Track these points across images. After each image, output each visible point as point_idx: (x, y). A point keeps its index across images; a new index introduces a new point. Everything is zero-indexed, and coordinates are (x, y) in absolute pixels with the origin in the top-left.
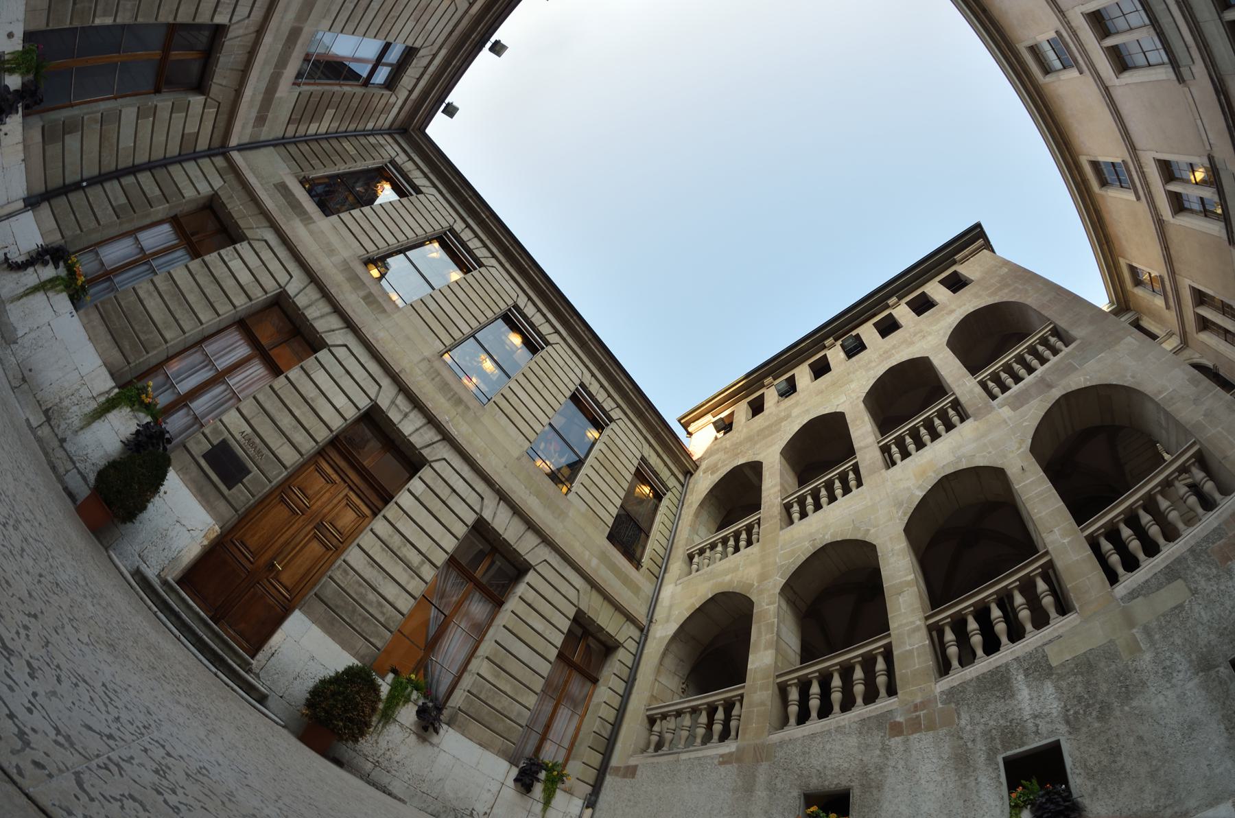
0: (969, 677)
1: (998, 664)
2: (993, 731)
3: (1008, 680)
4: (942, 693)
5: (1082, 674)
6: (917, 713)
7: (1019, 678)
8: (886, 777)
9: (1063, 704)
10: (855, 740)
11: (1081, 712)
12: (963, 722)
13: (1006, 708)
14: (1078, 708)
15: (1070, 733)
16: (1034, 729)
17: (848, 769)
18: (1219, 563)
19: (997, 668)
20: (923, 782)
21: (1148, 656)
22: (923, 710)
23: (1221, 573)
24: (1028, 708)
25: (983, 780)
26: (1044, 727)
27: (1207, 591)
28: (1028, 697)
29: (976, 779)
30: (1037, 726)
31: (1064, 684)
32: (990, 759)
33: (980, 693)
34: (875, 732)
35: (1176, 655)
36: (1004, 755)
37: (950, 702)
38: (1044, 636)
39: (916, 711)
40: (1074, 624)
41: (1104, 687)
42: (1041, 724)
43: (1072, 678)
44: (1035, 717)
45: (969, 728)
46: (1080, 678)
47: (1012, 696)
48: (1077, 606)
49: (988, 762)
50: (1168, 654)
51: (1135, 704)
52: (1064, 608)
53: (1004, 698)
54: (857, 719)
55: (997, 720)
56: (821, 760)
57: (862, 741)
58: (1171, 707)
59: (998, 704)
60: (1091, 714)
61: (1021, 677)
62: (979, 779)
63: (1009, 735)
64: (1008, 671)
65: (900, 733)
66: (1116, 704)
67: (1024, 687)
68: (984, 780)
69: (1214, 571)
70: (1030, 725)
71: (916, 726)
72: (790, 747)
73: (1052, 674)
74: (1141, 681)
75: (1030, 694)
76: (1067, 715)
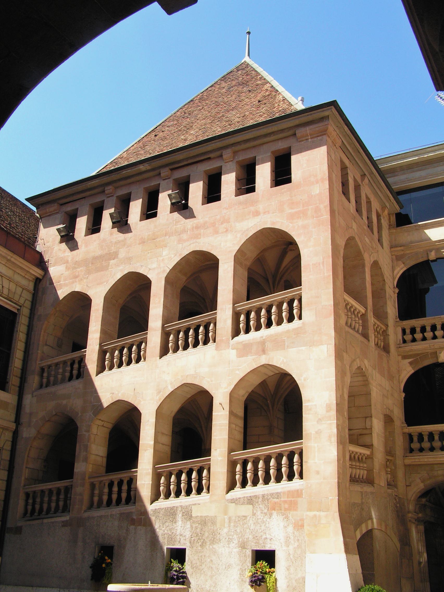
0: (162, 507)
2: (166, 535)
3: (176, 514)
6: (141, 517)
7: (179, 515)
9: (191, 534)
11: (196, 540)
13: (172, 527)
16: (179, 540)
18: (269, 509)
21: (226, 530)
22: (143, 516)
23: (268, 513)
24: (179, 530)
26: (182, 541)
28: (180, 525)
29: (156, 554)
30: (180, 539)
31: (194, 526)
35: (235, 536)
39: (141, 515)
41: (206, 534)
42: (182, 539)
43: (197, 525)
47: (175, 522)
50: (232, 534)
51: (214, 546)
54: (119, 512)
59: (170, 524)
60: (199, 542)
61: (180, 515)
62: (158, 554)
63: (170, 539)
67: (180, 520)
69: (266, 511)
70: (178, 537)
73: (191, 519)
75: (181, 524)
76: (191, 540)
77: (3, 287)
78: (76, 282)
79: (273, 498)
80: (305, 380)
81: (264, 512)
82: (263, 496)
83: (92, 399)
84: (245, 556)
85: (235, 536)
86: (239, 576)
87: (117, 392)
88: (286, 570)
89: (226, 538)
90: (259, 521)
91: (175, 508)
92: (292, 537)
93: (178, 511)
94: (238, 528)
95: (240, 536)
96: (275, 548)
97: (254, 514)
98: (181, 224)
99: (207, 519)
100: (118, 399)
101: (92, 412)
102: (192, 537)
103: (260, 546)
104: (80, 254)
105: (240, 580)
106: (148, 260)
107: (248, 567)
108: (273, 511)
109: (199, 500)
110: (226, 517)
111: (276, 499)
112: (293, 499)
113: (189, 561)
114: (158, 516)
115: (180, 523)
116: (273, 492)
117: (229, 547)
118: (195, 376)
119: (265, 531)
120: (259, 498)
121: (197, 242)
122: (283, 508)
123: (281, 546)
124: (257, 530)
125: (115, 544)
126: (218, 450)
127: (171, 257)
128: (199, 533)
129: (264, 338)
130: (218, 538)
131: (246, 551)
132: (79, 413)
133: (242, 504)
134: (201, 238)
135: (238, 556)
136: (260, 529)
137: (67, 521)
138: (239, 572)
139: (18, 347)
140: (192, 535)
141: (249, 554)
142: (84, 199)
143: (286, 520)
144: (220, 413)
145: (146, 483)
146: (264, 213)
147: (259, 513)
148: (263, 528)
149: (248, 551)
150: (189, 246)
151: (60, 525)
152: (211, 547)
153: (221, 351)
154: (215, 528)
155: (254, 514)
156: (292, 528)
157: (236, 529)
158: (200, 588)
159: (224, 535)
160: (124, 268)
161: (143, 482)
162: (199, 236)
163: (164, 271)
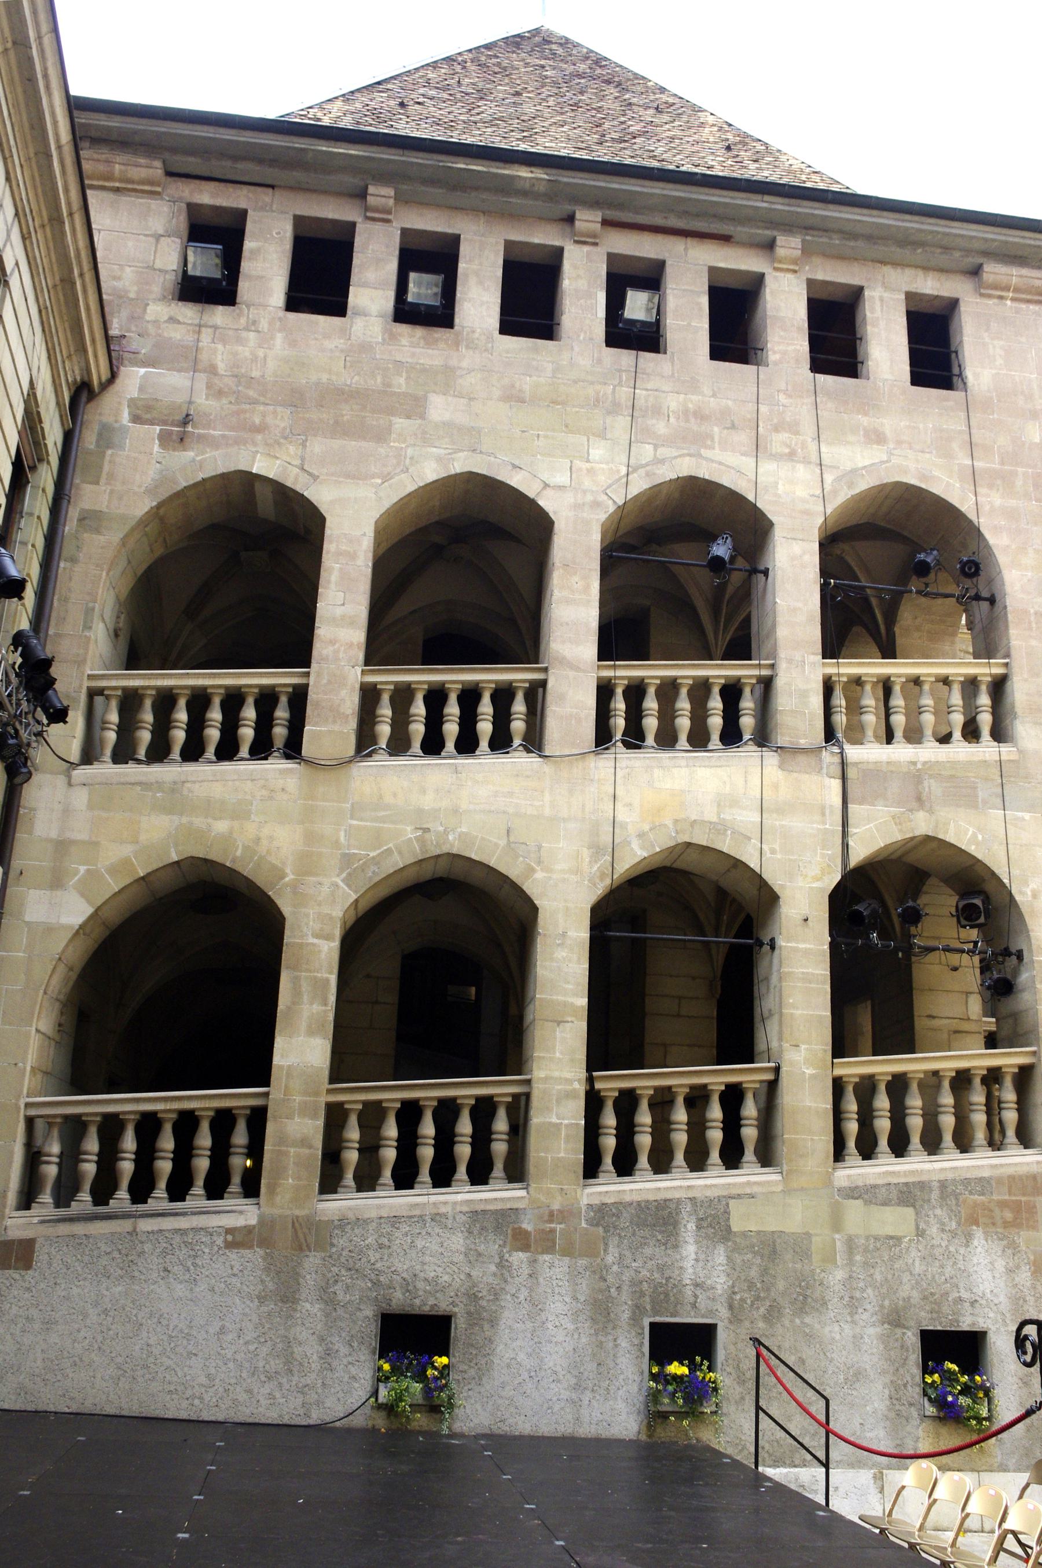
0: (628, 1198)
1: (669, 1196)
3: (676, 1224)
4: (590, 1206)
5: (762, 1256)
6: (553, 1226)
8: (502, 1307)
10: (461, 1241)
11: (749, 1301)
12: (610, 1259)
13: (665, 1259)
14: (746, 1295)
15: (731, 1322)
16: (692, 1300)
17: (450, 1285)
19: (665, 1200)
20: (550, 1325)
21: (840, 1275)
22: (560, 1223)
23: (959, 1233)
24: (690, 1271)
25: (624, 1343)
26: (703, 1302)
27: (934, 1242)
28: (693, 1256)
29: (615, 1340)
30: (696, 1296)
31: (738, 1259)
32: (635, 1320)
33: (638, 1225)
34: (491, 1236)
35: (870, 1291)
36: (652, 1320)
37: (597, 1225)
38: (734, 1185)
39: (551, 1221)
40: (774, 1189)
41: (781, 1285)
43: (749, 1256)
44: (697, 1285)
45: (615, 1268)
46: (758, 1261)
47: (676, 1247)
48: (785, 1168)
49: (632, 1322)
50: (861, 1284)
52: (766, 1157)
53: (665, 1244)
54: (465, 1209)
55: (651, 1271)
56: (408, 1264)
57: (473, 1246)
58: (843, 1343)
59: (657, 1250)
60: (758, 1308)
61: (691, 1226)
63: (662, 1297)
64: (678, 1212)
65: (525, 1248)
66: (788, 1310)
67: (691, 1240)
68: (623, 1345)
69: (954, 1225)
70: (688, 1291)
71: (546, 1243)
72: (356, 1231)
73: (728, 1240)
74: (823, 1298)
75: (696, 1253)
76: (732, 1298)
78: (255, 444)
79: (971, 1193)
80: (1035, 896)
81: (947, 1228)
82: (943, 1185)
83: (342, 834)
84: (902, 1347)
85: (870, 1291)
86: (888, 1403)
87: (441, 829)
88: (1021, 1385)
89: (842, 1298)
90: (937, 1252)
91: (673, 1206)
92: (1031, 1300)
93: (684, 1214)
94: (878, 1270)
95: (884, 1290)
96: (985, 1326)
97: (920, 1233)
98: (647, 390)
99: (778, 1241)
100: (445, 849)
101: (344, 875)
102: (734, 1293)
103: (943, 1320)
104: (265, 357)
105: (892, 1415)
106: (539, 456)
107: (913, 1377)
108: (974, 1228)
109: (749, 1183)
110: (837, 1236)
111: (979, 1195)
112: (1023, 1199)
113: (730, 1361)
114: (615, 1227)
115: (690, 1250)
116: (968, 1176)
117: (853, 1322)
118: (720, 827)
119: (955, 1280)
120: (931, 1190)
121: (700, 456)
122: (999, 1222)
123: (1004, 1321)
124: (933, 1277)
125: (456, 1310)
126: (803, 1047)
127: (618, 471)
128: (755, 1281)
129: (919, 766)
130: (817, 1294)
131: (904, 1334)
132: (288, 871)
133: (882, 1205)
134: (714, 448)
135: (882, 1347)
136: (942, 1274)
137: (248, 1230)
138: (887, 1391)
140: (733, 1287)
141: (913, 1340)
142: (270, 190)
143: (1009, 1251)
144: (802, 946)
145: (566, 1122)
146: (899, 443)
147: (934, 1230)
148: (949, 1271)
149: (909, 1334)
150: (676, 457)
151: (220, 1241)
152: (798, 1321)
153: (795, 775)
154: (806, 1267)
155: (920, 1233)
156: (1029, 1274)
157: (872, 1271)
158: (769, 1442)
159: (836, 1288)
160: (450, 454)
161: (554, 1120)
162: (709, 443)
163: (596, 504)
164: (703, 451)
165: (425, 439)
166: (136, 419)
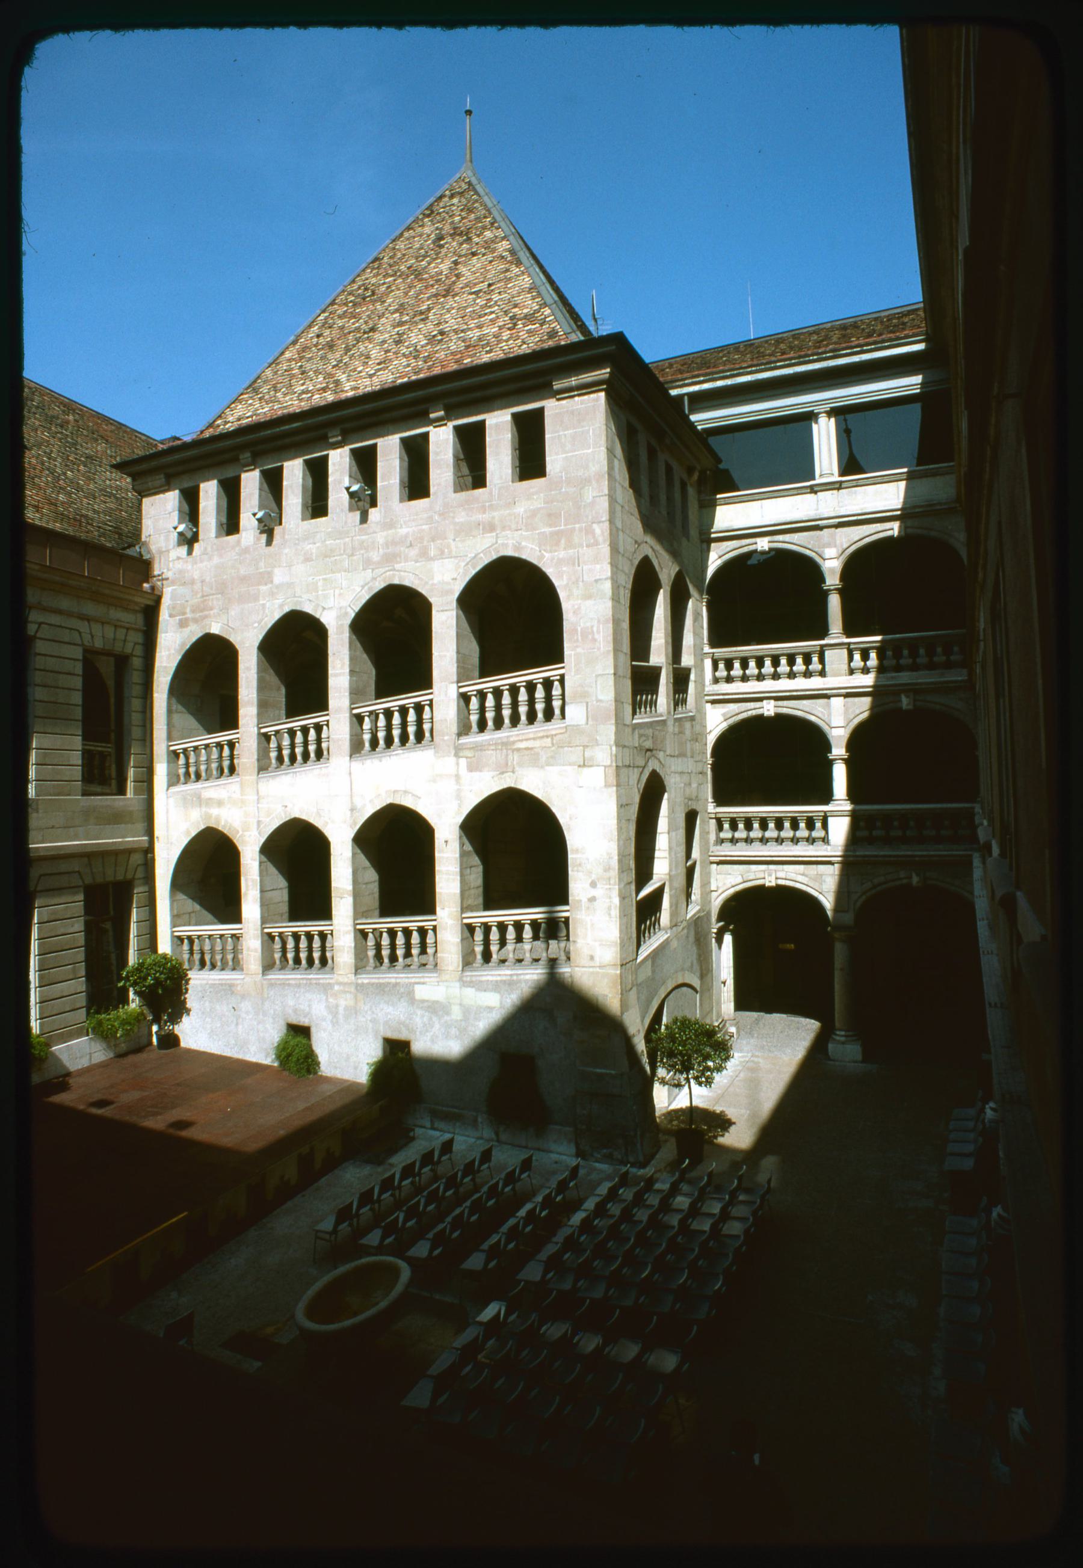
77: (92, 637)
121: (394, 570)
139: (134, 723)
146: (504, 528)
162: (398, 559)
164: (397, 566)
165: (272, 594)
166: (171, 616)
